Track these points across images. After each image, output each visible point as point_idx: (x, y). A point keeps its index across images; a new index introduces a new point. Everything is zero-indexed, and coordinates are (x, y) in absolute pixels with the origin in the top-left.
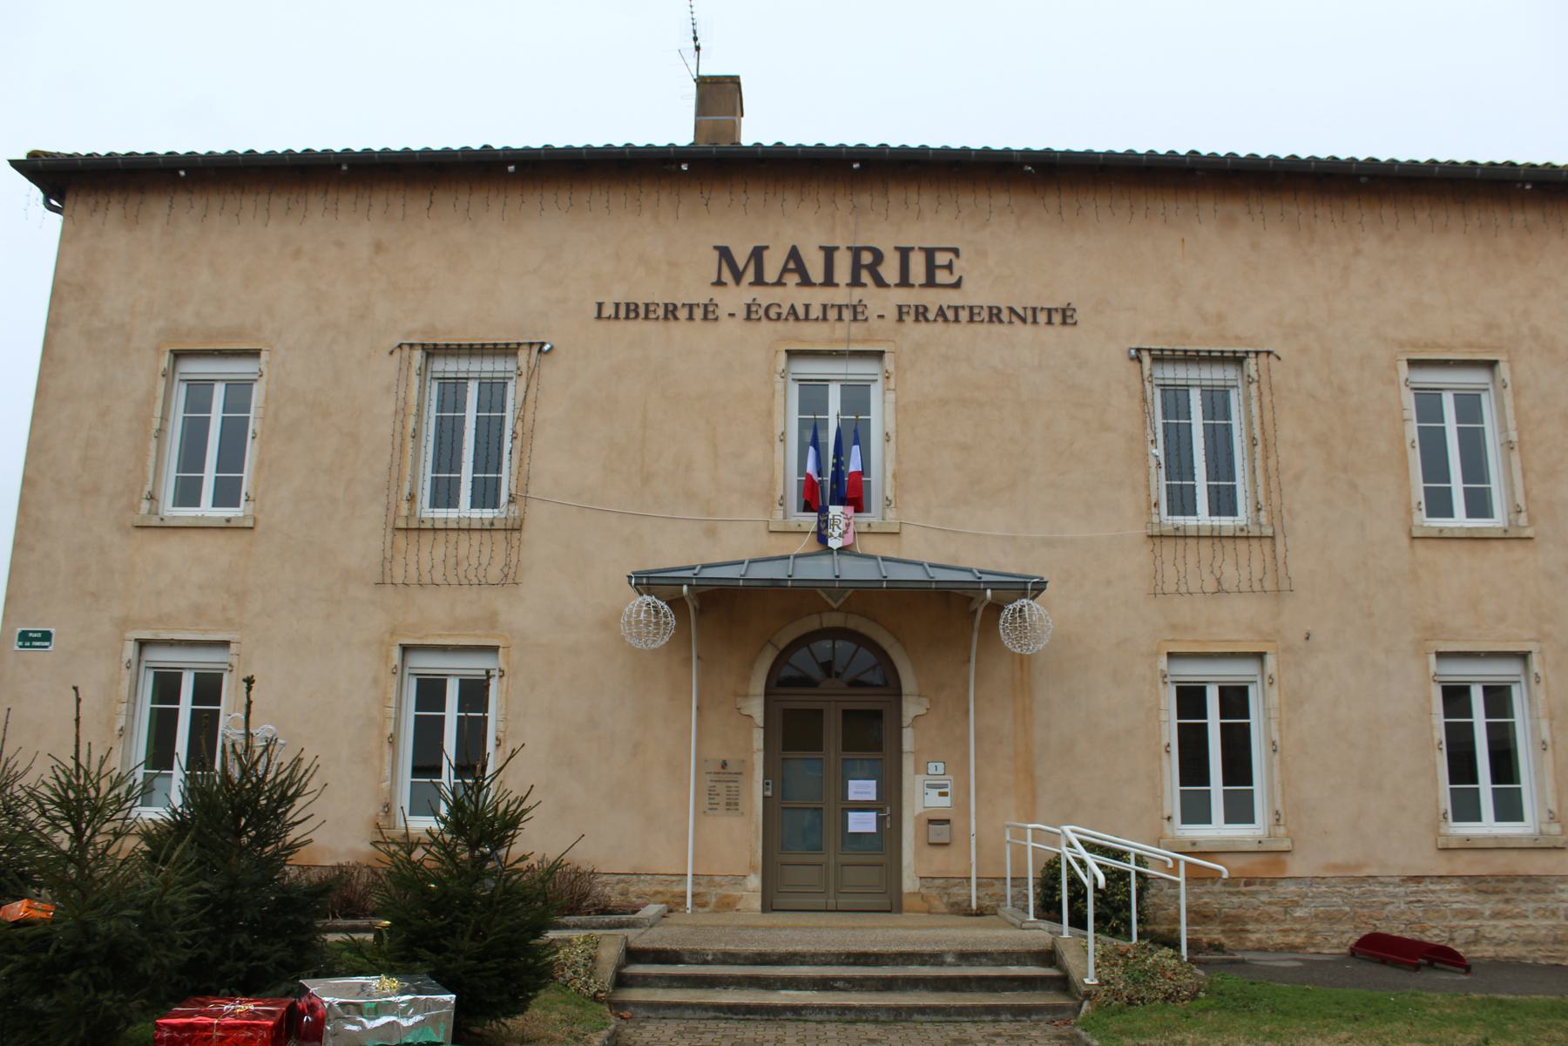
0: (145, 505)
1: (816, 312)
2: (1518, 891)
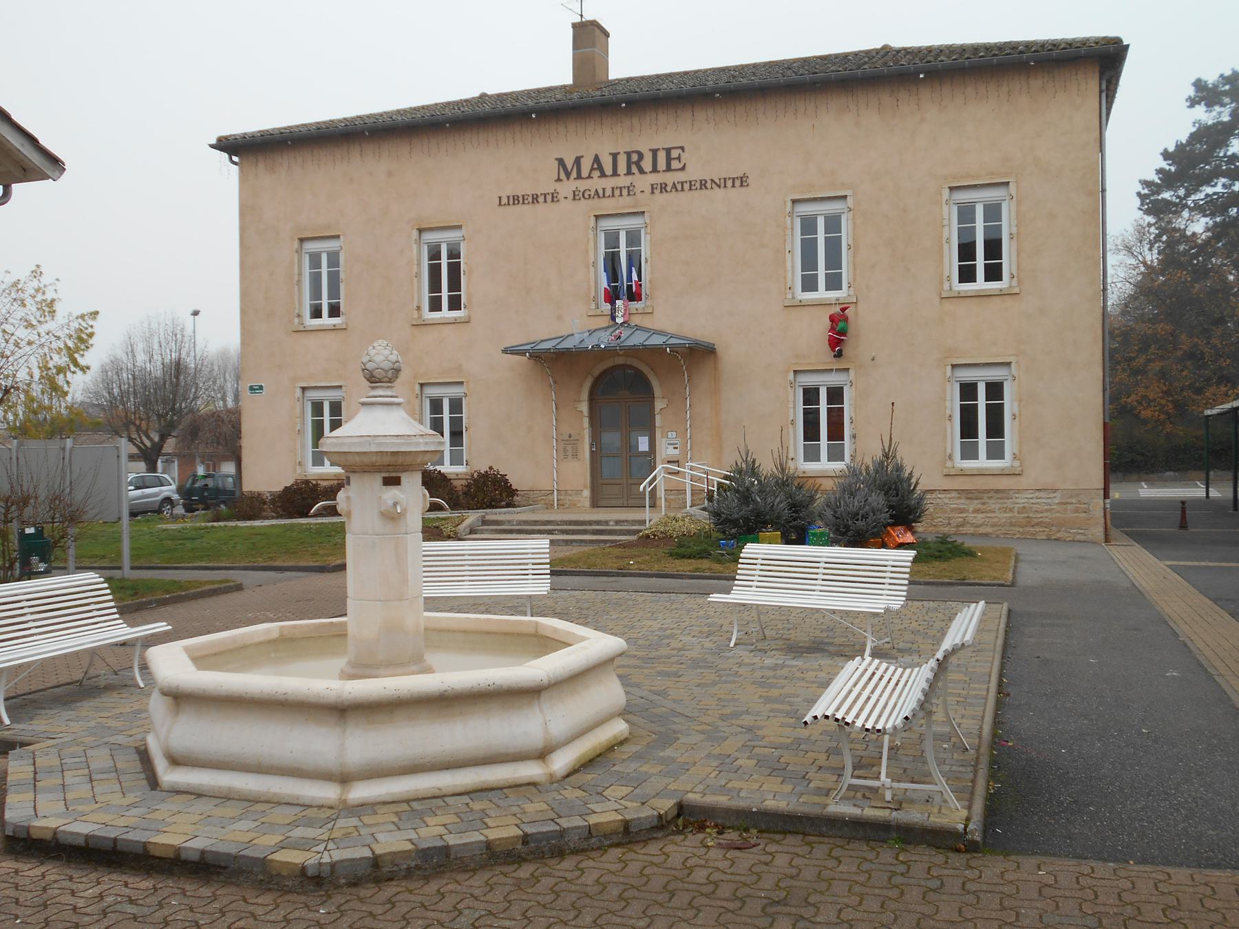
0: (296, 320)
1: (608, 192)
2: (991, 498)
